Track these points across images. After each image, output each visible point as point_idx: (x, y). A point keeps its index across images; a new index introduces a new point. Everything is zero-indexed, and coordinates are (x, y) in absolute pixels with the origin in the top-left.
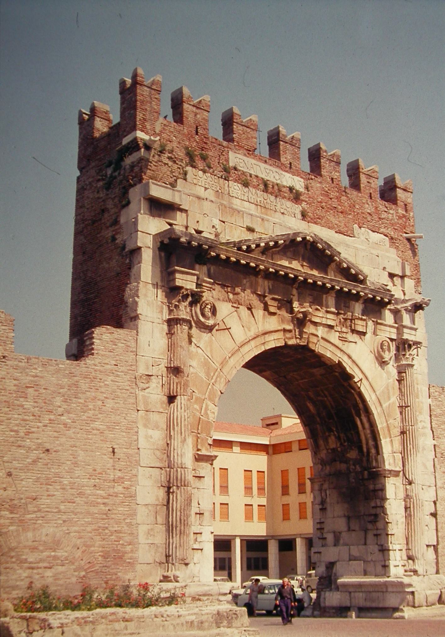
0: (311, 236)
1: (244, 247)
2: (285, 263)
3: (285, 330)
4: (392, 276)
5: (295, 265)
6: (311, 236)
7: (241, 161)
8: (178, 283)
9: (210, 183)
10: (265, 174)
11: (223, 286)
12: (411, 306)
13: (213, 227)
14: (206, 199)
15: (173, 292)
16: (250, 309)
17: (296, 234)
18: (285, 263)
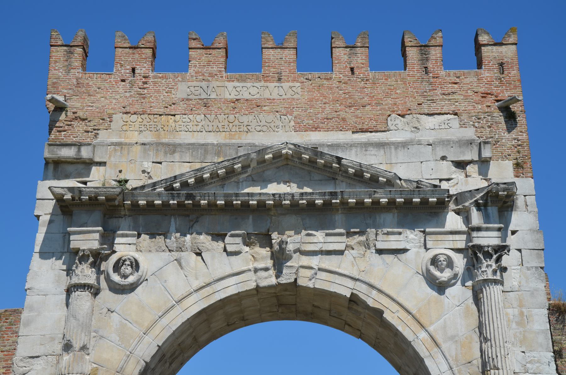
0: (290, 149)
1: (177, 185)
2: (256, 190)
3: (256, 270)
4: (461, 165)
5: (274, 188)
6: (290, 149)
7: (196, 88)
8: (73, 245)
9: (148, 124)
10: (234, 93)
11: (153, 235)
12: (482, 198)
13: (144, 172)
14: (136, 143)
15: (74, 257)
16: (199, 254)
17: (262, 151)
18: (256, 190)
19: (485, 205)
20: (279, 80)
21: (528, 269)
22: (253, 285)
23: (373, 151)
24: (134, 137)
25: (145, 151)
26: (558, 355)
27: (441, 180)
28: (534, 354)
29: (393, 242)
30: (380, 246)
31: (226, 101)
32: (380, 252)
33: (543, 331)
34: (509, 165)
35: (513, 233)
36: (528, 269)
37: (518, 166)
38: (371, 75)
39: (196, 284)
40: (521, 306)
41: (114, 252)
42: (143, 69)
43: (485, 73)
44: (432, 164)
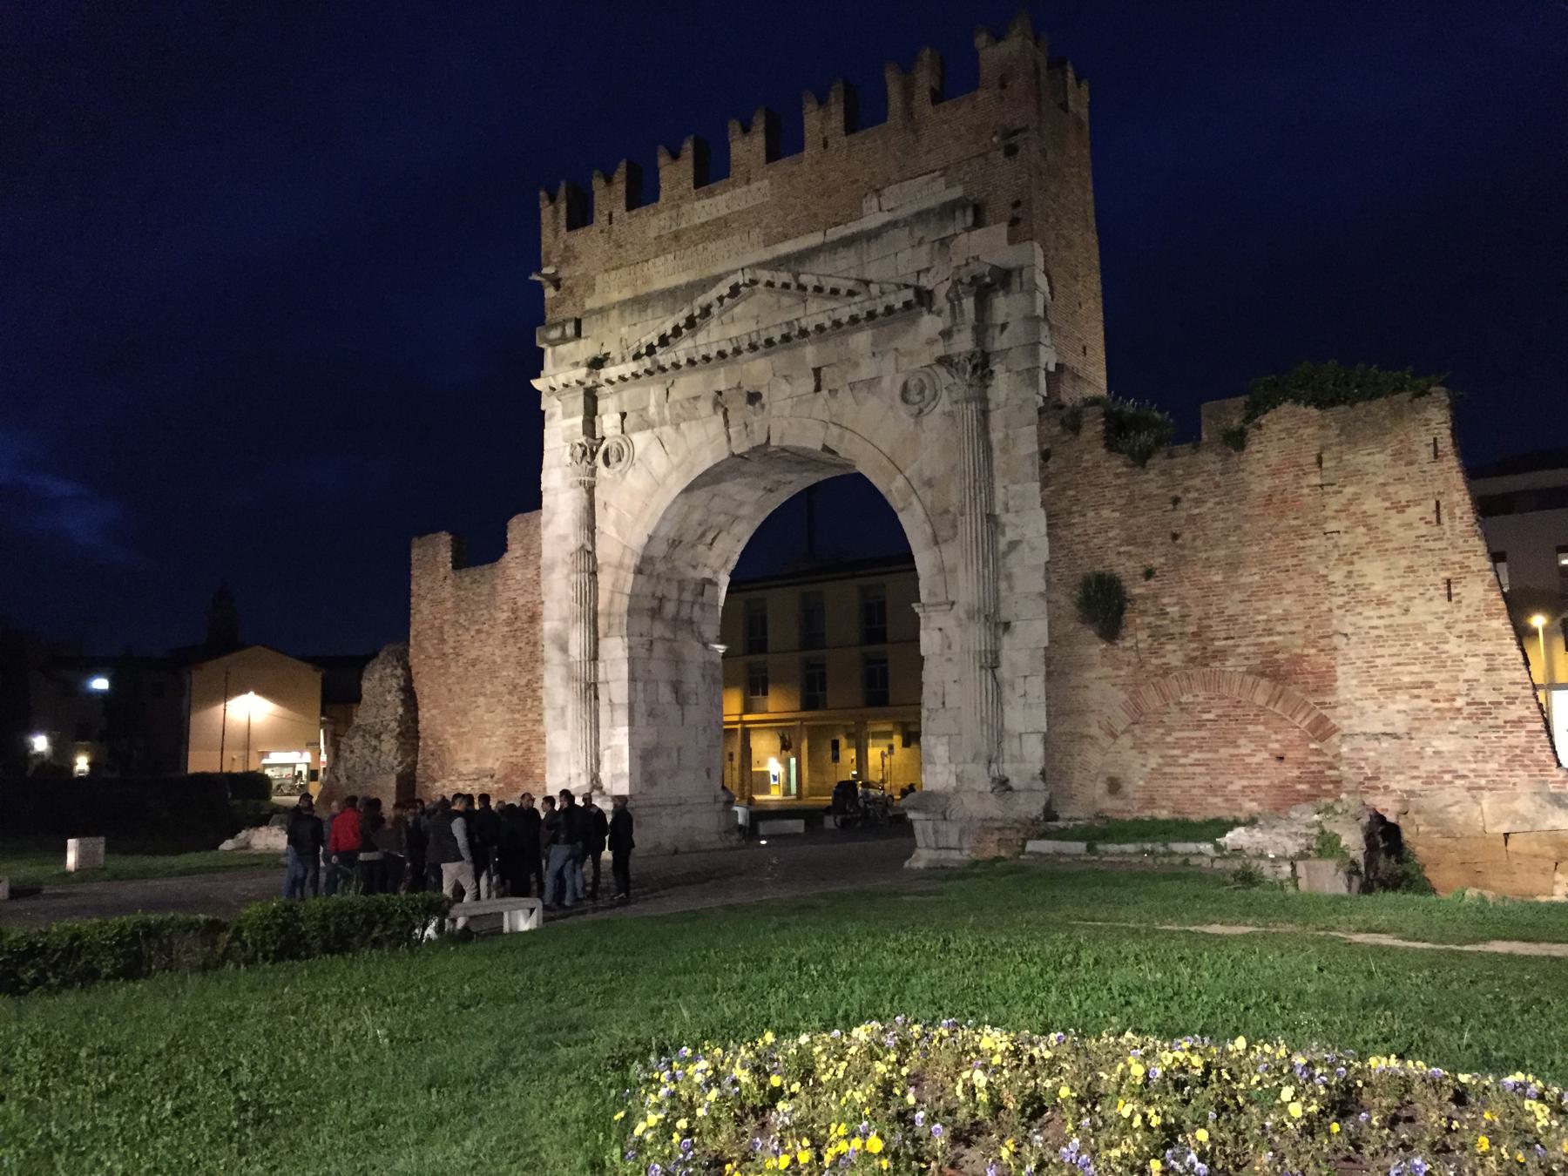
1: (643, 351)
19: (960, 299)
20: (748, 181)
21: (1018, 373)
22: (725, 455)
23: (842, 252)
24: (616, 297)
25: (622, 313)
26: (1045, 482)
27: (919, 273)
28: (1017, 487)
29: (866, 371)
30: (850, 378)
31: (696, 228)
32: (852, 386)
33: (1031, 456)
34: (1002, 229)
35: (1004, 327)
36: (1018, 373)
37: (1014, 222)
38: (845, 140)
39: (676, 460)
40: (1007, 426)
41: (603, 438)
42: (619, 210)
43: (982, 95)
44: (908, 253)
